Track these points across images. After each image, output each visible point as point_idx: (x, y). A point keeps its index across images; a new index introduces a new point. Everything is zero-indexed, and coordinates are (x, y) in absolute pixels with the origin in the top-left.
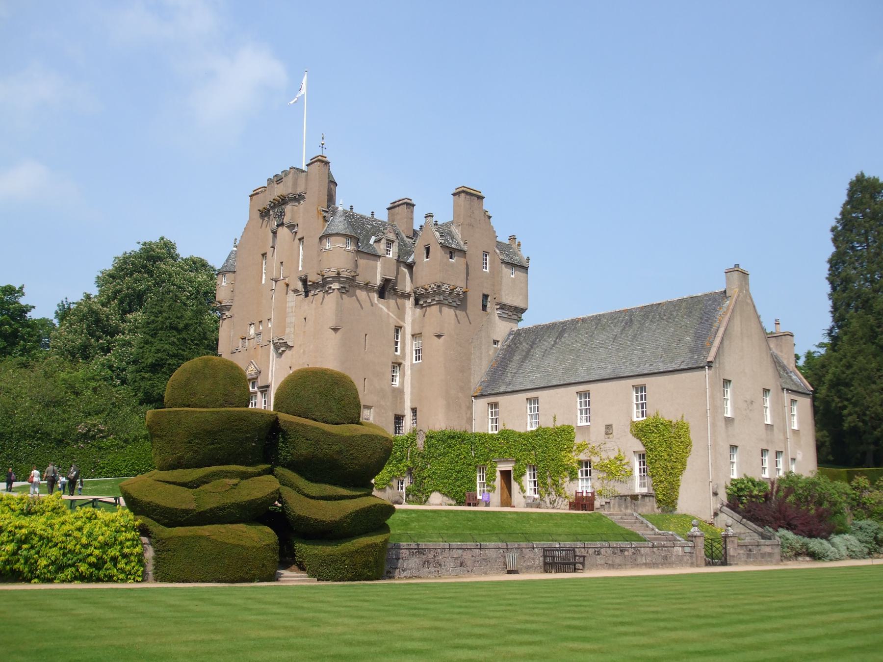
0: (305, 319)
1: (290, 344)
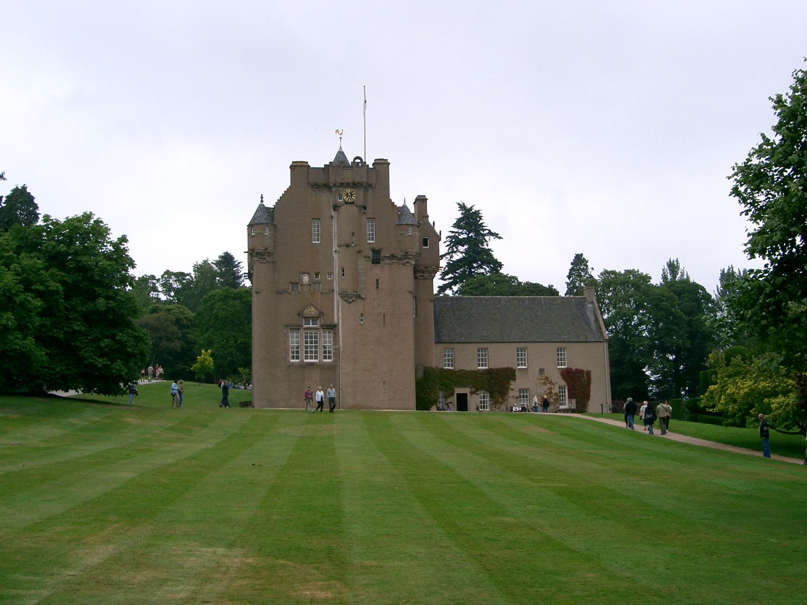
0: (377, 281)
1: (363, 297)
